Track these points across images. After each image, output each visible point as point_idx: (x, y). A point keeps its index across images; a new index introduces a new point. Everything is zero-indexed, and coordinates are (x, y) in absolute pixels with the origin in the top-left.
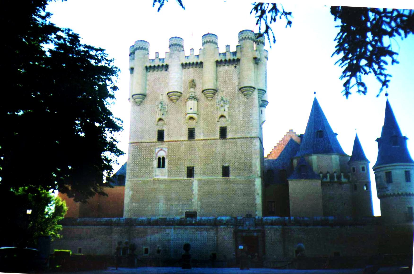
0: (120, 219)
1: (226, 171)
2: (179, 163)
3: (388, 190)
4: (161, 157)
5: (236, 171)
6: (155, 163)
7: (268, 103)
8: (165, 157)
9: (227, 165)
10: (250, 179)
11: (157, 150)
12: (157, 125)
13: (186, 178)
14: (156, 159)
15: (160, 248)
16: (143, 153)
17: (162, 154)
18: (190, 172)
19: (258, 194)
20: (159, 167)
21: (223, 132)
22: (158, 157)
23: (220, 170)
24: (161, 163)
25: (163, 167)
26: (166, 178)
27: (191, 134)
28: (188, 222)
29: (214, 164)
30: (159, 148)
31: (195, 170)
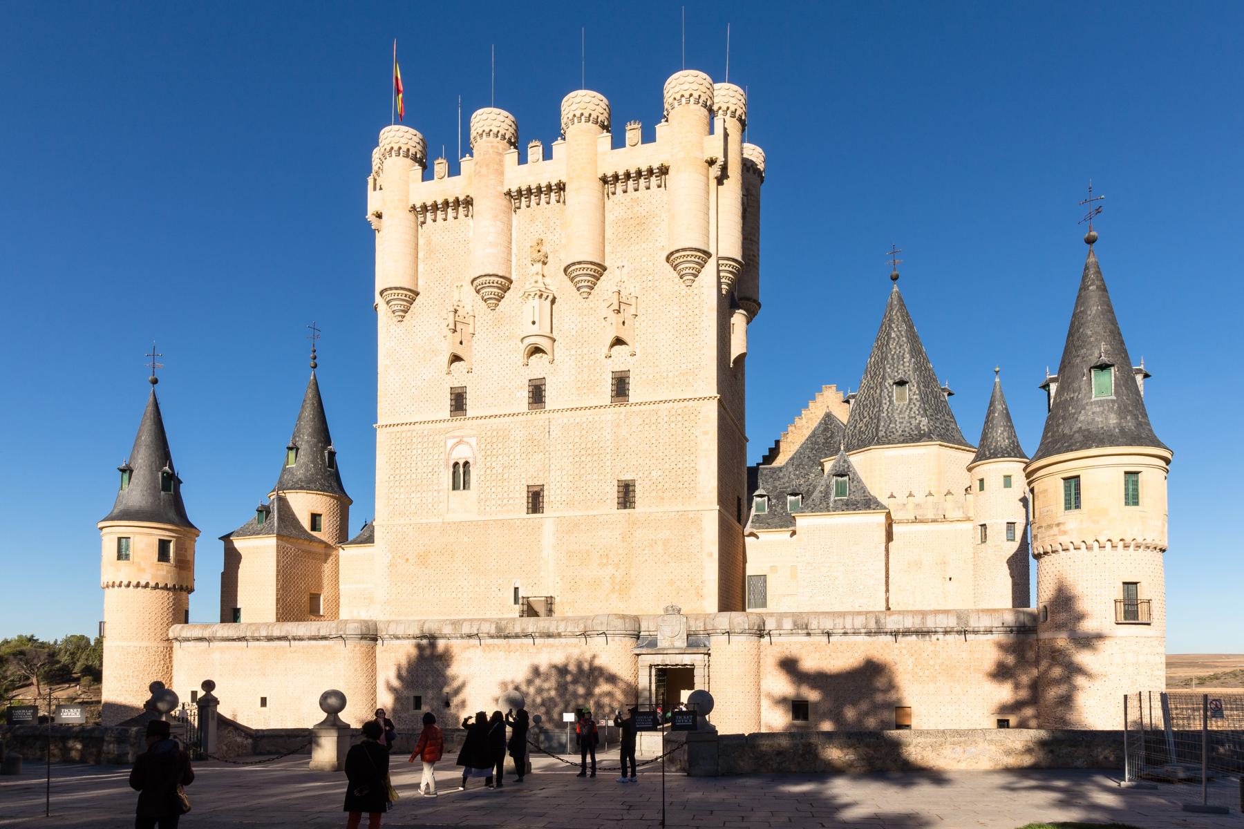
1: (626, 495)
2: (506, 476)
3: (1065, 532)
4: (461, 463)
5: (654, 494)
7: (759, 305)
8: (470, 461)
9: (627, 477)
10: (691, 515)
11: (450, 443)
14: (447, 466)
17: (461, 454)
19: (711, 555)
20: (455, 487)
21: (621, 387)
23: (613, 493)
24: (461, 475)
27: (537, 394)
29: (595, 477)
31: (546, 493)
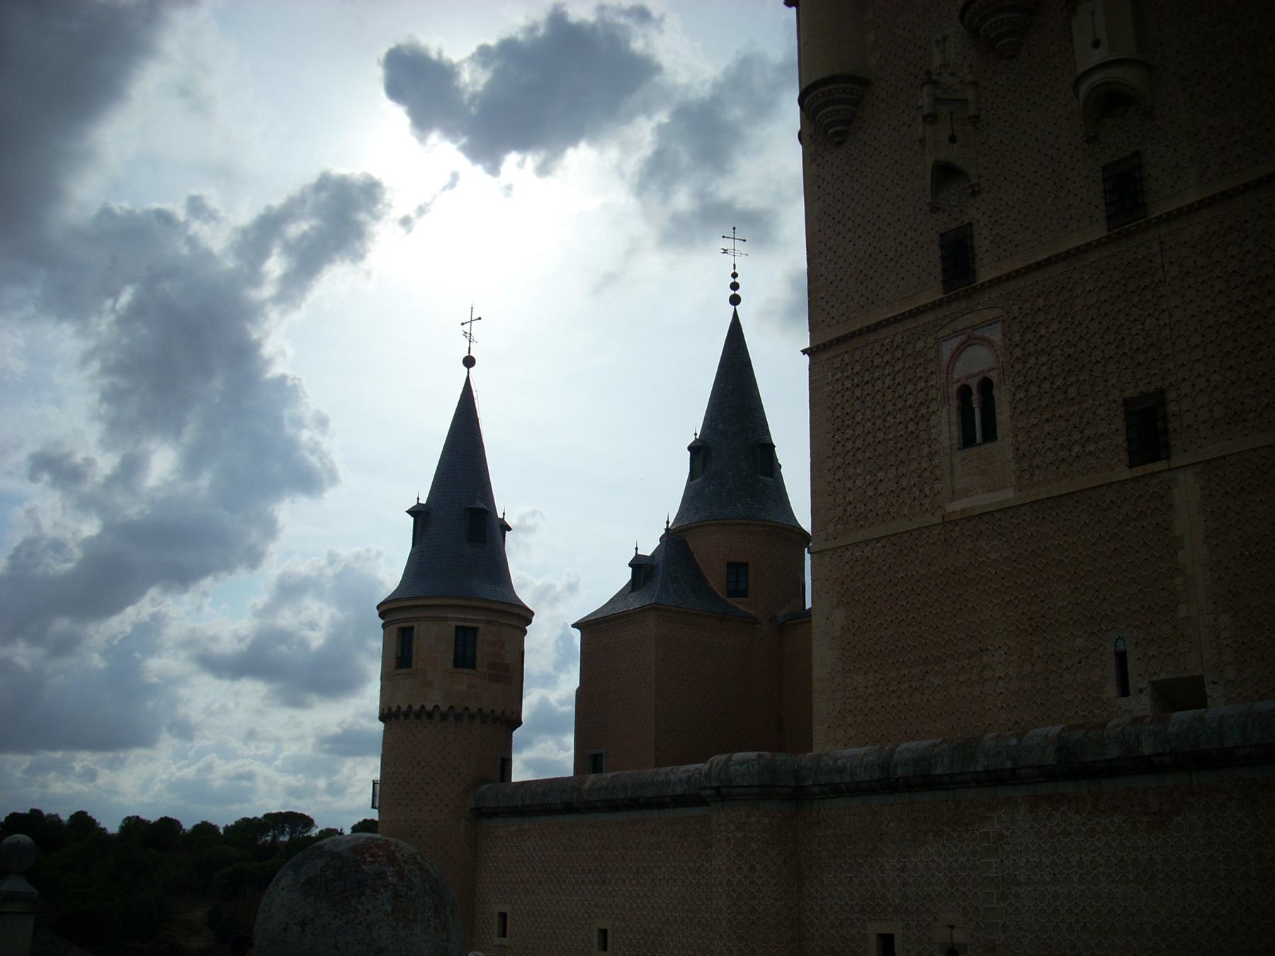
0: (729, 759)
2: (1072, 392)
4: (974, 383)
6: (946, 426)
8: (993, 376)
11: (947, 349)
12: (934, 209)
13: (1123, 473)
15: (959, 936)
16: (879, 385)
18: (1148, 431)
20: (967, 440)
22: (956, 387)
24: (976, 414)
25: (990, 434)
26: (1008, 495)
28: (1113, 752)
30: (955, 333)
31: (1173, 408)
